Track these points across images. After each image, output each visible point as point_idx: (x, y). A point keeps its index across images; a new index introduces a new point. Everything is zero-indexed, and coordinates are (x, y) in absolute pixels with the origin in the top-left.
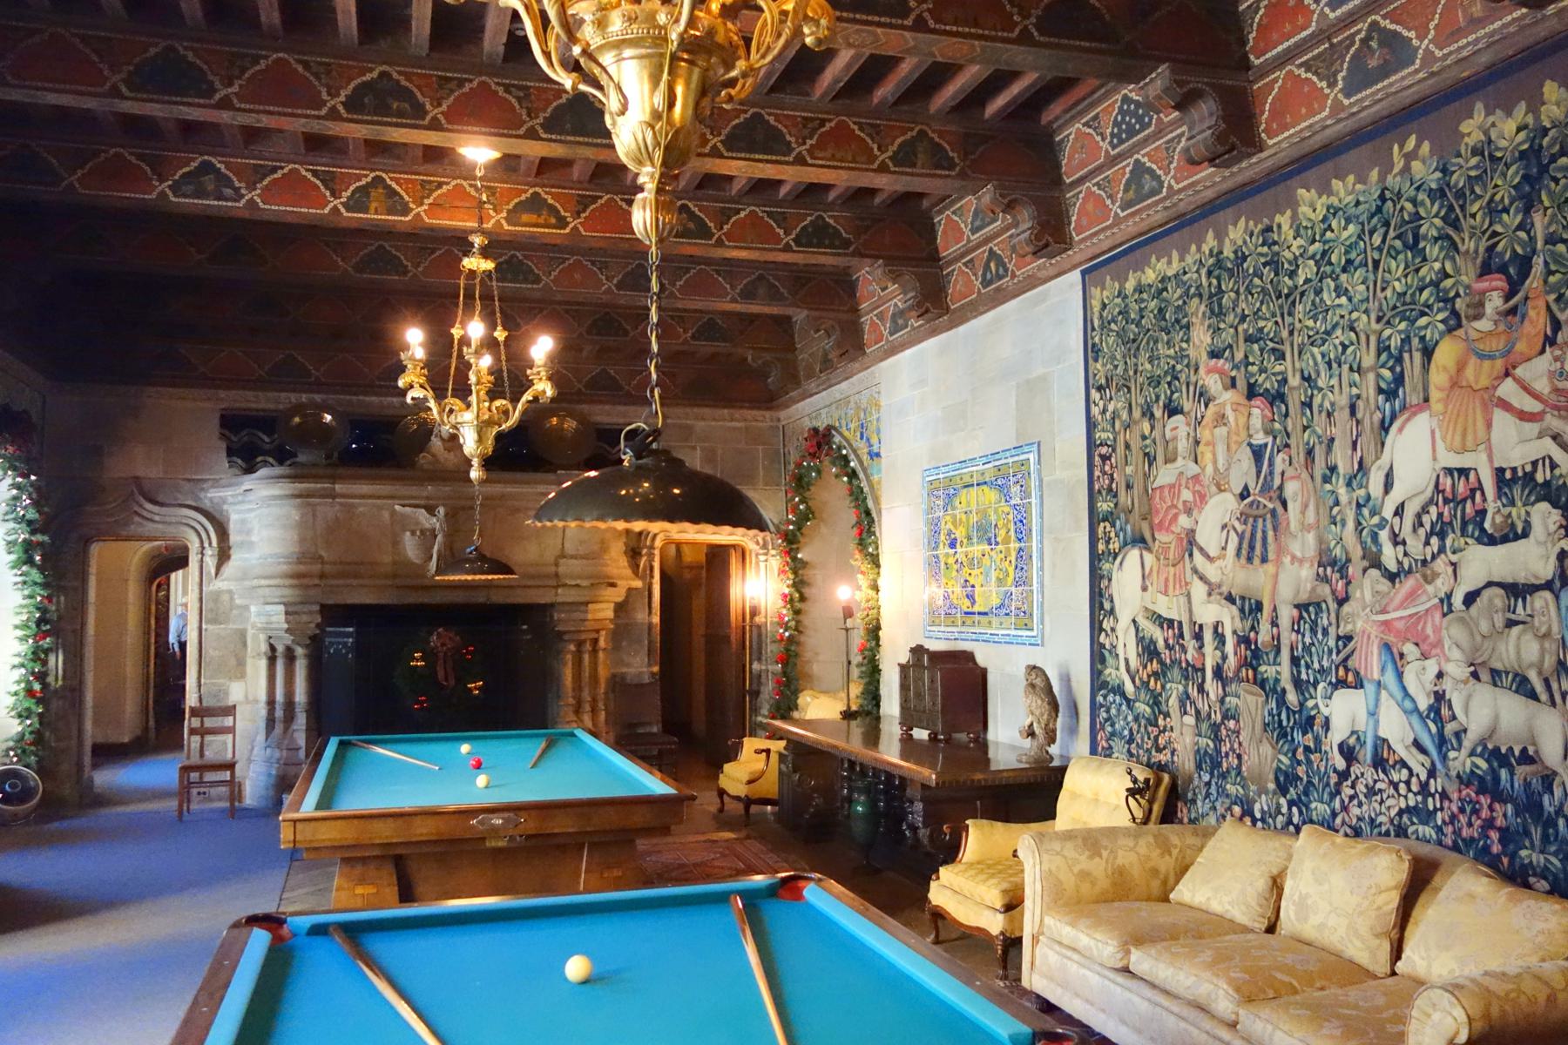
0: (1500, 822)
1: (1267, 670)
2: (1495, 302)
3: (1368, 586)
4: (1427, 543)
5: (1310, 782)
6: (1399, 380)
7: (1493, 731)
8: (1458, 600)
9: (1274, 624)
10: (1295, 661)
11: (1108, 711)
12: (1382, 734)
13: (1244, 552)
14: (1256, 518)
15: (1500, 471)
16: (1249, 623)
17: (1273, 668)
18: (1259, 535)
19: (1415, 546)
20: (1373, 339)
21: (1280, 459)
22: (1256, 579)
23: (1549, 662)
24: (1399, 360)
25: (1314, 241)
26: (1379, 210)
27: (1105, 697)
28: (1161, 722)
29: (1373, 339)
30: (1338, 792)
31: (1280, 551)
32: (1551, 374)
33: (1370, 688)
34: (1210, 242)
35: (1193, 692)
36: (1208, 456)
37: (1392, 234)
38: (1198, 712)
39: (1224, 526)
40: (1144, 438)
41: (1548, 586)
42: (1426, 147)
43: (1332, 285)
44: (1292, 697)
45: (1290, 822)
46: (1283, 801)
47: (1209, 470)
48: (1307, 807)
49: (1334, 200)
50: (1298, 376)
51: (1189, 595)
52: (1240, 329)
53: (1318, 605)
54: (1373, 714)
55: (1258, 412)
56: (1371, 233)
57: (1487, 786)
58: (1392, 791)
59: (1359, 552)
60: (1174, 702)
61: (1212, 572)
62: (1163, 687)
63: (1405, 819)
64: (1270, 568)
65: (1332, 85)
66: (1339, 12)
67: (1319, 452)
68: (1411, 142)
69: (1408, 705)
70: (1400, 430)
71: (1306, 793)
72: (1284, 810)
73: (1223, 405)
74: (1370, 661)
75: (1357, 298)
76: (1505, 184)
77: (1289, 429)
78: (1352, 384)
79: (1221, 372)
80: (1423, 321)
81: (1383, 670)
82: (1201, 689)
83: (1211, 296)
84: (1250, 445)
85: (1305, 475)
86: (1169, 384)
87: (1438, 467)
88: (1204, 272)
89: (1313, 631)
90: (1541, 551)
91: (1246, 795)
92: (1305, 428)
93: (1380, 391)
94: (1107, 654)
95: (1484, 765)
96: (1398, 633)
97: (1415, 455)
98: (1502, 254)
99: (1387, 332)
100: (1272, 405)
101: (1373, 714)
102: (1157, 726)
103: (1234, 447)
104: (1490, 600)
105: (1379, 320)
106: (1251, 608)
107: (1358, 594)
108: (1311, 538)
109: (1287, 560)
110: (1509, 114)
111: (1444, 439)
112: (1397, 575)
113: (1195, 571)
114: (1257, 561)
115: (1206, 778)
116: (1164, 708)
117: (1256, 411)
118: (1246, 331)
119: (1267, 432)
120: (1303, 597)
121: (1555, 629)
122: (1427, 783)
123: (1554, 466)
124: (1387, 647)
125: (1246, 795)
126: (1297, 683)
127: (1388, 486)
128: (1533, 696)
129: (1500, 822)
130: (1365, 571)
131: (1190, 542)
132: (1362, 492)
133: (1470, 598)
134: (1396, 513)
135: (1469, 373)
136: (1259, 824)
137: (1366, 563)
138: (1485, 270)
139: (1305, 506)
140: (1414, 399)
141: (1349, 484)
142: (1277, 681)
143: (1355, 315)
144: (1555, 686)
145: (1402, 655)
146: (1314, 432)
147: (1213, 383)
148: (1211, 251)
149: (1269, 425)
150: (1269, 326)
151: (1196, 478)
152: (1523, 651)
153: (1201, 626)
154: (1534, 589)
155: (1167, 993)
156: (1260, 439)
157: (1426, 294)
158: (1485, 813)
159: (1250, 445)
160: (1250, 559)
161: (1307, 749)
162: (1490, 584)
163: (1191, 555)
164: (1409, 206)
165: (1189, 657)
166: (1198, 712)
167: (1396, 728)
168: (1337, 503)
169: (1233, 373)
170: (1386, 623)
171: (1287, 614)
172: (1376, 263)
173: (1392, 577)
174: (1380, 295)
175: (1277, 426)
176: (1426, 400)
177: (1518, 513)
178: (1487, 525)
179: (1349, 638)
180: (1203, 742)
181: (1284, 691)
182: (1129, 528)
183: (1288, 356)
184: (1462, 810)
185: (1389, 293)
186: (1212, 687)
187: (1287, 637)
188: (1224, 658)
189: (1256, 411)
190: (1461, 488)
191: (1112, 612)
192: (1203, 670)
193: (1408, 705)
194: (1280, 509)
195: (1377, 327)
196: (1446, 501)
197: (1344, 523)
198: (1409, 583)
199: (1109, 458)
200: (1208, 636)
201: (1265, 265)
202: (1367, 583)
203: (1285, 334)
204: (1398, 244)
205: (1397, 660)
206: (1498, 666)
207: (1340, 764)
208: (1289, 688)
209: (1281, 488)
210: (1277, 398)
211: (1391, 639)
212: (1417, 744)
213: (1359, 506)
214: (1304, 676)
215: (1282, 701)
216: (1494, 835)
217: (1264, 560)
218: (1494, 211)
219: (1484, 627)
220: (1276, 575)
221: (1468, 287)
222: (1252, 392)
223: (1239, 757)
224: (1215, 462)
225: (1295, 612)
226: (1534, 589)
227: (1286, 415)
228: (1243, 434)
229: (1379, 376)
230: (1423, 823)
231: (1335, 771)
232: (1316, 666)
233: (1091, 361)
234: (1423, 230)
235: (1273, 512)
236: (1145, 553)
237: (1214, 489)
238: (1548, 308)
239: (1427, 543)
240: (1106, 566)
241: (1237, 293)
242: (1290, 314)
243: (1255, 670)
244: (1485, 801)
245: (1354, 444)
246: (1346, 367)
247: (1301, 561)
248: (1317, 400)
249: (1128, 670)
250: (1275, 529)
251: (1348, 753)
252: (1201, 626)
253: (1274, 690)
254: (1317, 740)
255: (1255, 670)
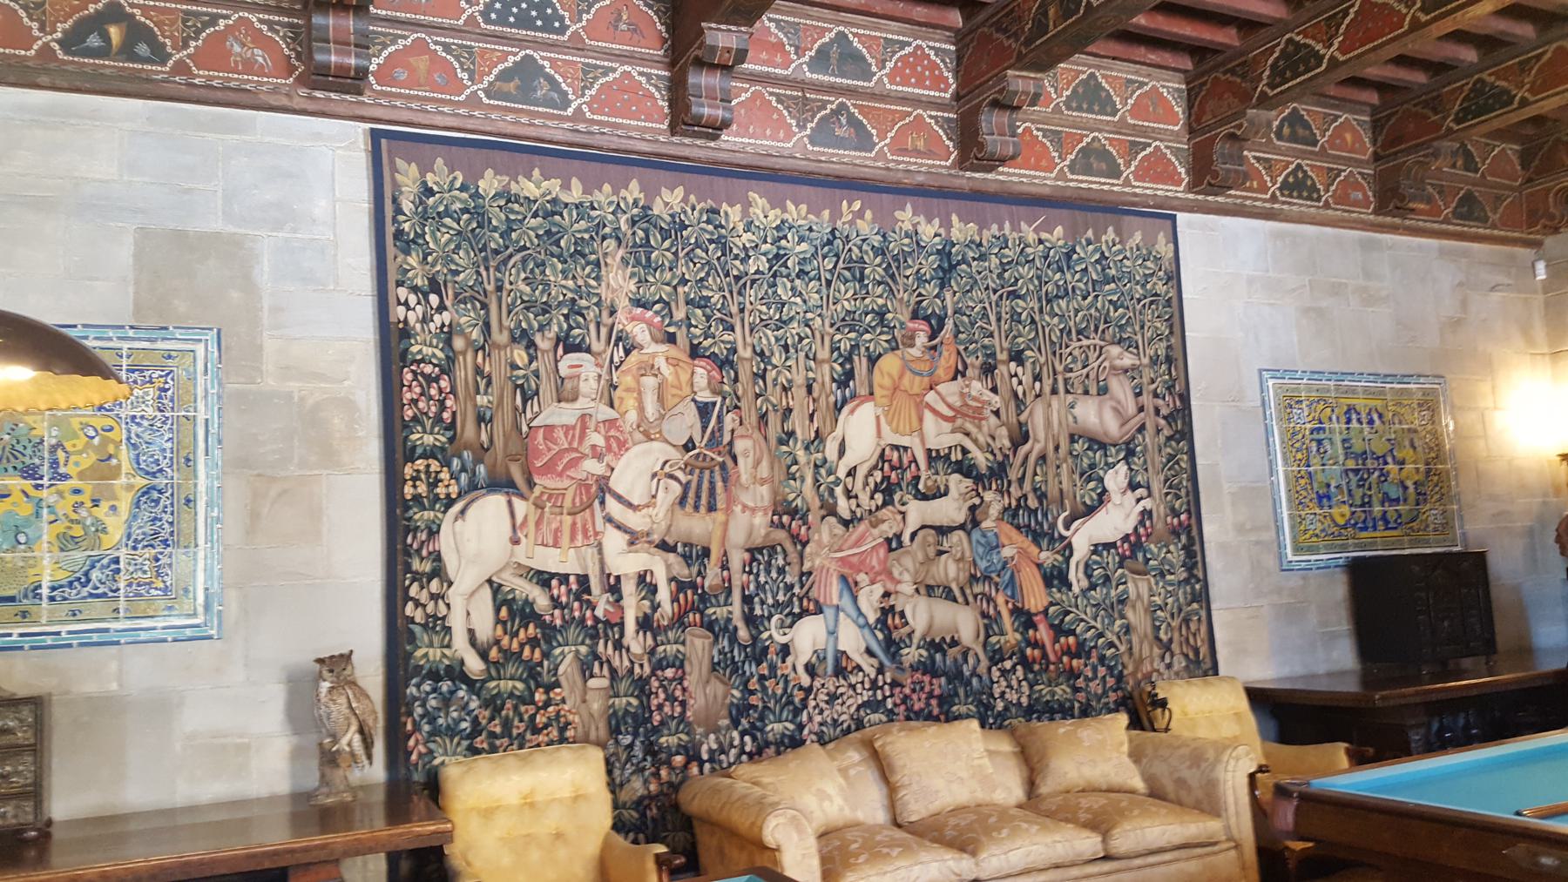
0: (937, 692)
1: (717, 612)
2: (922, 339)
3: (825, 532)
4: (872, 498)
5: (766, 708)
6: (850, 375)
7: (930, 627)
8: (906, 538)
9: (725, 566)
10: (747, 600)
11: (423, 705)
12: (841, 648)
13: (691, 500)
14: (702, 470)
15: (929, 451)
16: (695, 569)
17: (725, 609)
18: (706, 485)
19: (864, 498)
20: (827, 339)
21: (730, 420)
22: (697, 526)
23: (963, 577)
24: (849, 359)
25: (765, 242)
26: (829, 242)
27: (418, 686)
28: (539, 696)
29: (827, 339)
30: (805, 707)
31: (731, 501)
32: (962, 395)
33: (829, 612)
34: (633, 191)
35: (605, 649)
36: (630, 403)
37: (841, 264)
38: (613, 671)
39: (654, 475)
40: (514, 367)
41: (962, 527)
42: (868, 214)
43: (789, 285)
44: (743, 633)
45: (743, 752)
46: (735, 734)
47: (632, 416)
48: (762, 730)
49: (786, 216)
50: (749, 349)
51: (600, 545)
52: (680, 289)
53: (773, 547)
54: (832, 633)
55: (702, 373)
56: (824, 257)
57: (927, 668)
58: (851, 692)
59: (818, 503)
60: (568, 667)
61: (635, 521)
62: (546, 655)
63: (862, 713)
64: (719, 516)
65: (802, 127)
66: (815, 76)
67: (774, 420)
68: (857, 205)
69: (861, 621)
70: (852, 412)
71: (762, 718)
72: (736, 742)
73: (654, 355)
74: (832, 592)
75: (811, 303)
76: (929, 264)
77: (740, 393)
78: (808, 369)
79: (650, 324)
80: (867, 336)
81: (841, 597)
82: (618, 645)
83: (635, 245)
84: (694, 400)
85: (757, 435)
86: (566, 317)
87: (883, 443)
88: (623, 219)
89: (768, 572)
90: (956, 505)
91: (692, 741)
92: (758, 396)
93: (834, 380)
94: (417, 629)
95: (925, 653)
96: (851, 566)
97: (860, 434)
98: (926, 309)
99: (838, 337)
100: (721, 368)
101: (832, 633)
102: (533, 702)
103: (670, 401)
104: (924, 538)
105: (832, 325)
106: (696, 554)
107: (816, 537)
108: (765, 491)
109: (738, 509)
110: (929, 221)
111: (890, 424)
112: (851, 521)
113: (609, 519)
114: (703, 509)
115: (627, 740)
116: (546, 678)
117: (699, 370)
118: (687, 294)
119: (714, 392)
120: (758, 542)
121: (968, 554)
122: (876, 679)
123: (965, 451)
124: (843, 578)
125: (692, 741)
126: (750, 620)
127: (842, 452)
128: (955, 600)
129: (937, 692)
130: (823, 518)
131: (603, 488)
132: (819, 455)
133: (914, 535)
134: (849, 474)
135: (906, 382)
136: (707, 766)
137: (823, 512)
138: (915, 316)
139: (757, 463)
140: (863, 391)
141: (807, 448)
142: (729, 620)
143: (809, 315)
144: (968, 591)
145: (856, 583)
146: (767, 400)
147: (640, 333)
148: (636, 202)
149: (718, 387)
150: (716, 297)
151: (611, 423)
152: (949, 570)
153: (618, 578)
154: (951, 529)
155: (1057, 867)
156: (705, 396)
157: (869, 317)
158: (927, 689)
159: (694, 400)
160: (696, 508)
161: (762, 678)
162: (923, 527)
163: (602, 503)
164: (855, 249)
165: (599, 613)
166: (613, 671)
167: (852, 640)
168: (796, 463)
169: (671, 330)
170: (841, 559)
171: (737, 559)
172: (829, 283)
173: (846, 524)
174: (832, 307)
175: (726, 388)
176: (872, 394)
177: (941, 479)
178: (921, 487)
179: (810, 573)
180: (620, 702)
181: (736, 629)
182: (481, 469)
183: (738, 328)
184: (914, 691)
185: (839, 307)
186: (636, 643)
187: (738, 579)
188: (655, 607)
189: (699, 370)
190: (905, 461)
191: (438, 572)
192: (622, 625)
193: (861, 621)
194: (730, 463)
195: (831, 331)
196: (893, 468)
197: (803, 480)
198: (862, 527)
199: (437, 379)
200: (628, 588)
201: (711, 241)
202: (825, 528)
203: (734, 309)
204: (847, 273)
205: (850, 587)
206: (932, 582)
207: (805, 680)
208: (740, 624)
209: (731, 444)
210: (725, 363)
211: (846, 571)
212: (869, 652)
213: (816, 466)
214: (758, 612)
215: (733, 639)
216: (934, 702)
217: (712, 508)
218: (920, 279)
219: (920, 556)
220: (726, 524)
221: (902, 324)
222: (695, 352)
223: (683, 704)
224: (641, 409)
225: (747, 556)
226: (951, 529)
227: (736, 380)
228: (687, 390)
229: (832, 368)
230: (874, 712)
231: (801, 688)
232: (770, 601)
233: (391, 250)
234: (867, 272)
235: (723, 466)
236: (516, 501)
237: (638, 436)
238: (959, 353)
239: (872, 498)
240: (421, 517)
241: (675, 254)
242: (740, 293)
243: (702, 613)
244: (927, 679)
245: (811, 416)
246: (802, 355)
247: (754, 510)
248: (771, 375)
249: (473, 640)
250: (725, 480)
251: (810, 669)
252: (618, 578)
253: (725, 629)
254: (773, 668)
255: (702, 613)
